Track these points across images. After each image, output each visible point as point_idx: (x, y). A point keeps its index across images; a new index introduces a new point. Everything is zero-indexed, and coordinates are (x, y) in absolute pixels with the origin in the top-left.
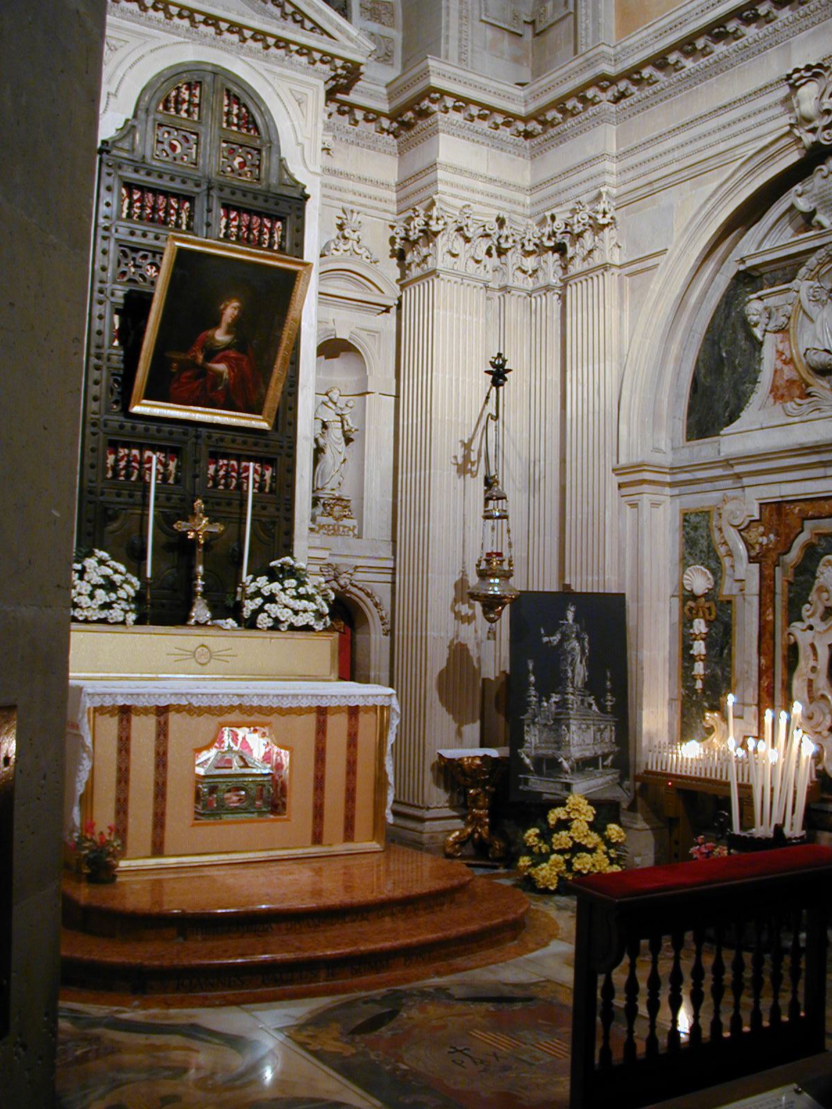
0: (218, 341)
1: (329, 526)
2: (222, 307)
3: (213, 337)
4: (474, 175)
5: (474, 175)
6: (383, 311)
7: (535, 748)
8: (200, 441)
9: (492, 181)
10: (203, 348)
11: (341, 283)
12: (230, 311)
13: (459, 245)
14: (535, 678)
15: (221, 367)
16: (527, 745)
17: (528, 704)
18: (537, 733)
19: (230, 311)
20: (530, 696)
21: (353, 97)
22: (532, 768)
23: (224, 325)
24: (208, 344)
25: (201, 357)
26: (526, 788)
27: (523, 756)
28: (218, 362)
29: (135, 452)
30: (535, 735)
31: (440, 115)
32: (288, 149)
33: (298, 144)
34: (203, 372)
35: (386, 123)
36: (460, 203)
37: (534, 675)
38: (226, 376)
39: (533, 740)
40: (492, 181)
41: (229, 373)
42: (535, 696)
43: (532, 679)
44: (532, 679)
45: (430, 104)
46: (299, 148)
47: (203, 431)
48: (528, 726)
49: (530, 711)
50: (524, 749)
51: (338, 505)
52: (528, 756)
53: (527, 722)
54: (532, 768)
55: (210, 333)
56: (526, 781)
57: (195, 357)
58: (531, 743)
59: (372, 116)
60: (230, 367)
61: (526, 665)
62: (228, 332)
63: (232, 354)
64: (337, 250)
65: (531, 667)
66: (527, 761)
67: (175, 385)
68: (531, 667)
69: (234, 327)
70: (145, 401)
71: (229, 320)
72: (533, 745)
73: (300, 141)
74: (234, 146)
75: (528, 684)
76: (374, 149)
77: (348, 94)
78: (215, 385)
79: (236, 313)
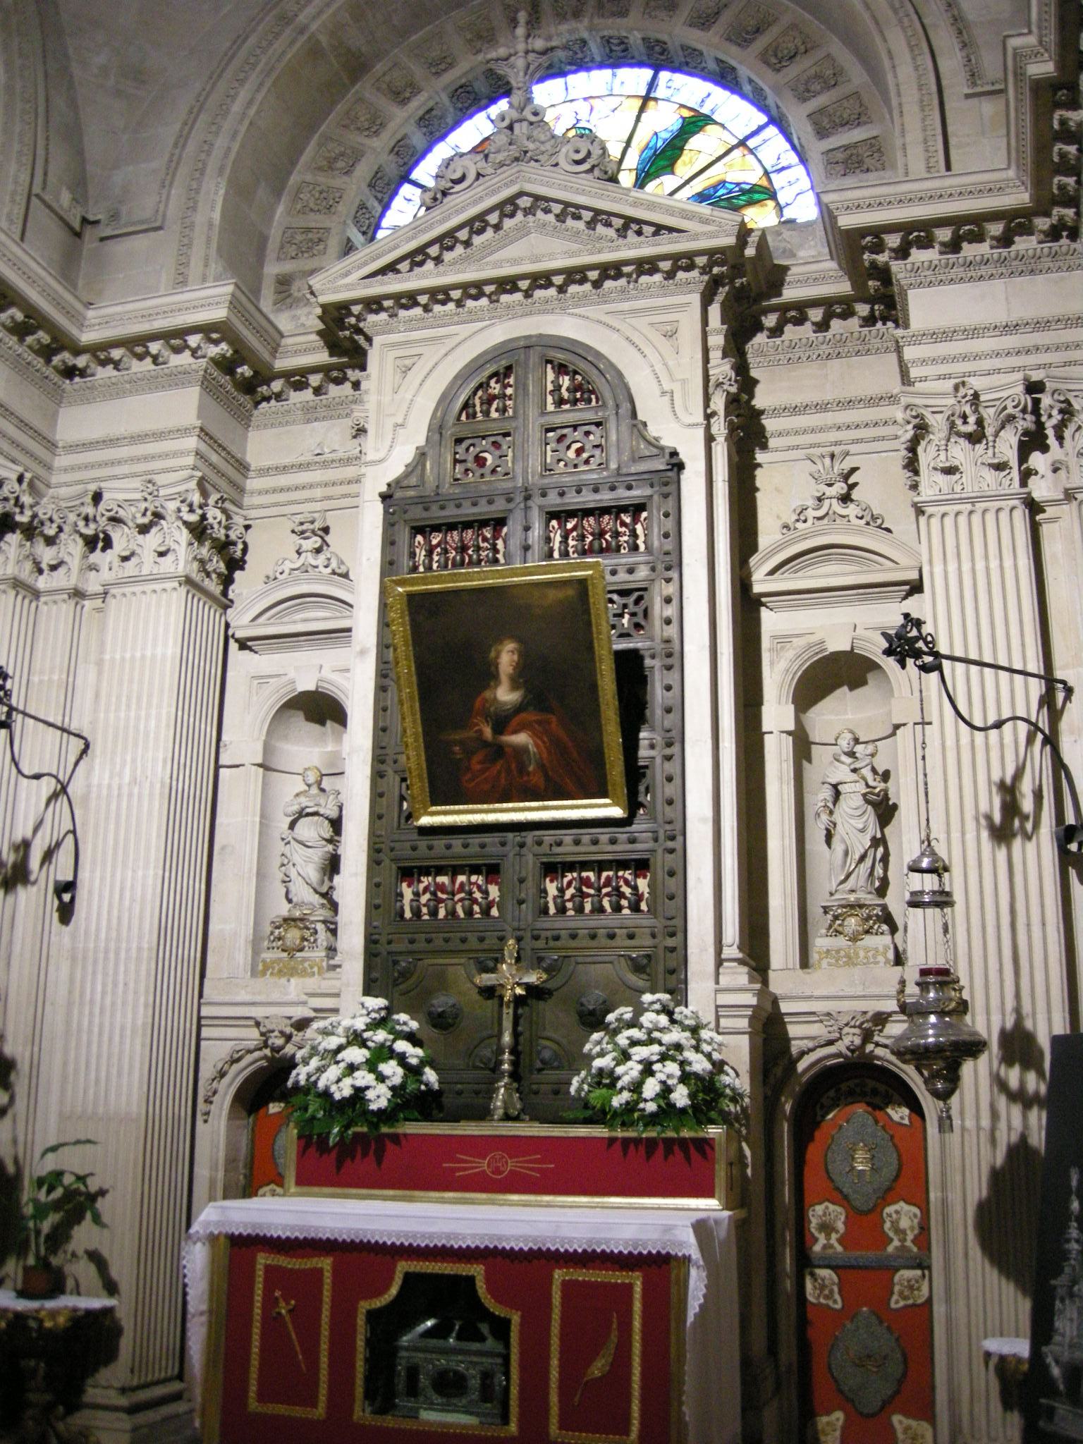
0: (505, 703)
1: (838, 951)
2: (493, 654)
3: (495, 699)
4: (973, 332)
5: (973, 332)
6: (909, 594)
7: (1071, 1346)
8: (524, 850)
9: (1010, 328)
10: (487, 716)
11: (832, 568)
12: (507, 657)
13: (960, 452)
14: (1081, 1204)
15: (522, 738)
16: (1057, 1338)
17: (1065, 1256)
18: (1075, 1316)
19: (507, 657)
20: (1068, 1241)
21: (790, 293)
22: (1062, 1387)
23: (504, 678)
24: (492, 709)
25: (488, 732)
26: (1051, 1428)
27: (1049, 1360)
28: (515, 732)
29: (591, 875)
30: (1071, 1320)
31: (896, 267)
32: (650, 407)
33: (664, 393)
34: (499, 751)
35: (863, 309)
36: (948, 385)
37: (1078, 1197)
38: (532, 748)
39: (1068, 1329)
40: (1010, 328)
41: (536, 745)
42: (1077, 1241)
43: (1075, 1205)
44: (1075, 1205)
45: (874, 256)
46: (667, 398)
47: (530, 837)
48: (1062, 1300)
49: (1067, 1270)
50: (1052, 1347)
51: (852, 915)
52: (1057, 1362)
53: (1061, 1292)
54: (1062, 1387)
55: (487, 694)
56: (1051, 1412)
57: (480, 732)
58: (1063, 1335)
59: (836, 308)
60: (535, 735)
61: (1069, 1179)
62: (514, 686)
63: (530, 716)
64: (805, 521)
65: (1074, 1183)
66: (1056, 1371)
67: (469, 776)
68: (1074, 1183)
69: (521, 677)
70: (434, 808)
71: (510, 670)
72: (1067, 1340)
73: (667, 387)
74: (565, 431)
75: (1066, 1215)
76: (868, 352)
77: (780, 295)
78: (522, 769)
79: (516, 657)
